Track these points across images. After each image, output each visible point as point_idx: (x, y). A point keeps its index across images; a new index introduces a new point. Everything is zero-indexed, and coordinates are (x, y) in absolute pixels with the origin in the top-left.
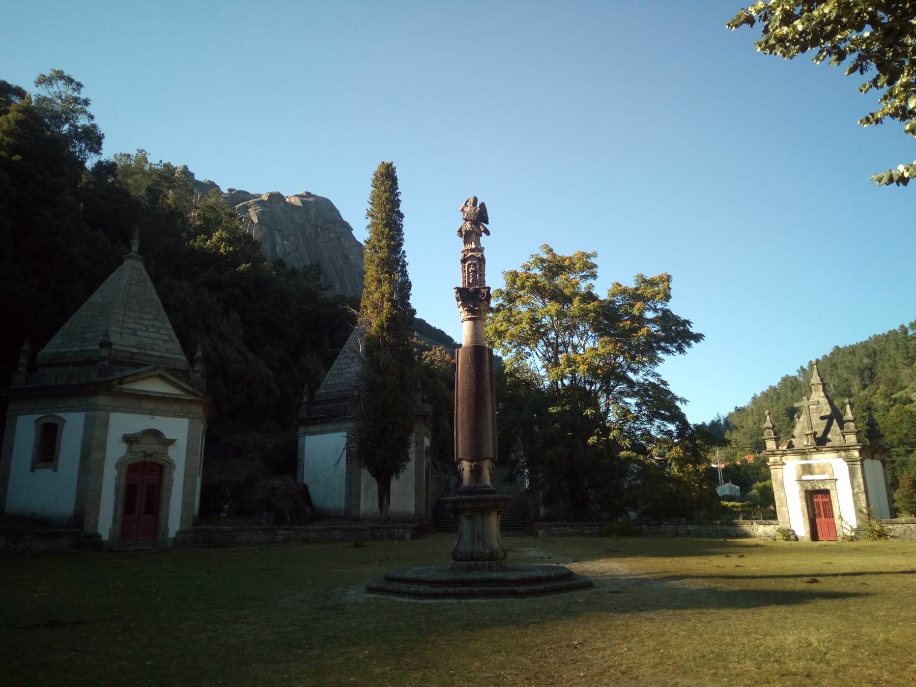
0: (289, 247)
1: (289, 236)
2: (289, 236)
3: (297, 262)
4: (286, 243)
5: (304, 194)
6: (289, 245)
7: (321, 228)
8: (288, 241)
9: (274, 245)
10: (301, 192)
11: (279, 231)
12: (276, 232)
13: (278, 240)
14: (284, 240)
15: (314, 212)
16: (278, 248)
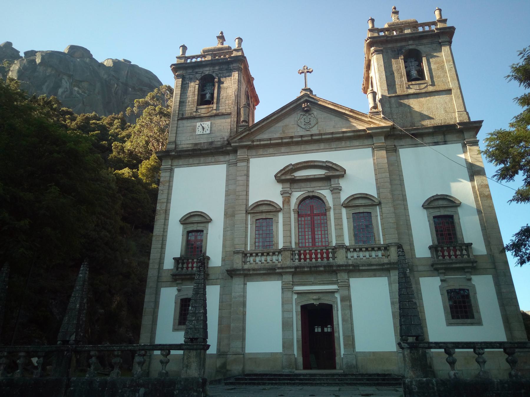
0: (79, 93)
1: (81, 81)
2: (81, 81)
3: (80, 105)
4: (76, 89)
5: (122, 61)
6: (80, 92)
7: (133, 88)
8: (79, 88)
9: (57, 86)
10: (121, 59)
11: (70, 76)
12: (66, 78)
13: (65, 83)
14: (75, 86)
15: (126, 72)
16: (60, 91)
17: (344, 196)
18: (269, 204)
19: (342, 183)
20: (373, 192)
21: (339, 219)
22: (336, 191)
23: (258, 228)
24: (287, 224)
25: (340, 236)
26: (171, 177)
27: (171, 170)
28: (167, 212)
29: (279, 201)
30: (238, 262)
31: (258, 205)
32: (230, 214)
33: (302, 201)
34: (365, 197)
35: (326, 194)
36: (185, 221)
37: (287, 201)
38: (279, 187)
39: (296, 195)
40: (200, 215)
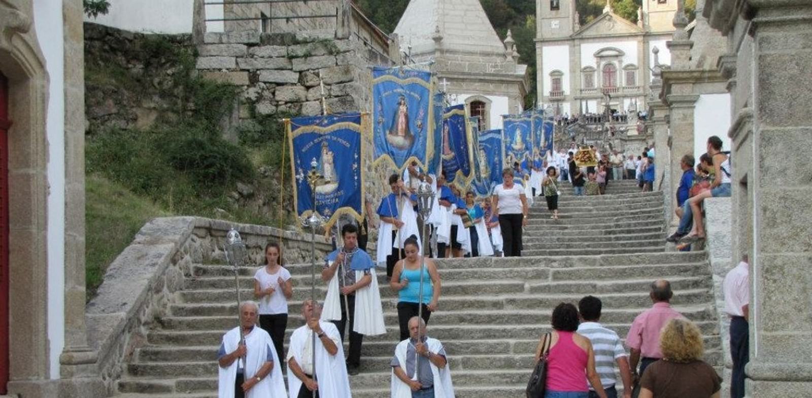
17: (624, 65)
18: (591, 67)
19: (623, 58)
20: (635, 62)
21: (621, 74)
22: (621, 62)
23: (586, 79)
24: (599, 75)
25: (621, 82)
26: (542, 51)
27: (541, 48)
28: (542, 69)
29: (595, 66)
30: (578, 95)
31: (585, 68)
32: (572, 71)
33: (605, 65)
34: (632, 65)
35: (615, 62)
36: (553, 74)
37: (598, 66)
38: (595, 60)
39: (603, 63)
40: (559, 72)
